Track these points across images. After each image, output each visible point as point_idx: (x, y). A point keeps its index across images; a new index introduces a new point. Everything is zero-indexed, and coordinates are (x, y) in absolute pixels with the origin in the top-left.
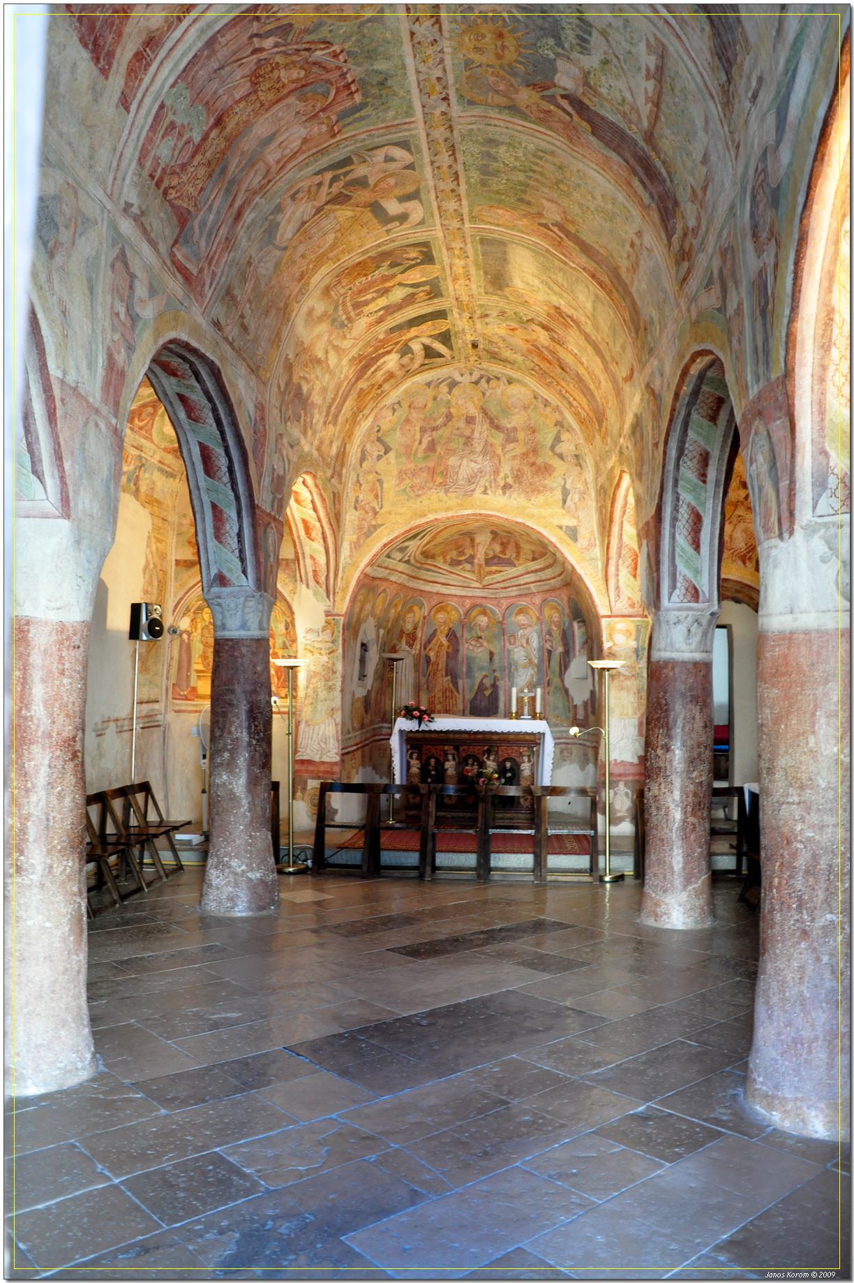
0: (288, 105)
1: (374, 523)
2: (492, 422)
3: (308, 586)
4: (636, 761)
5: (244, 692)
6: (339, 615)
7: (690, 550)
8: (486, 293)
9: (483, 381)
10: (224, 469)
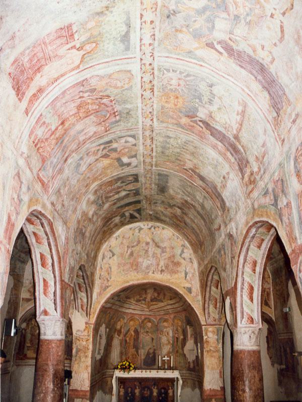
0: (90, 119)
1: (107, 285)
3: (78, 311)
4: (219, 389)
5: (53, 365)
6: (91, 324)
7: (249, 301)
8: (157, 194)
9: (153, 228)
10: (50, 264)
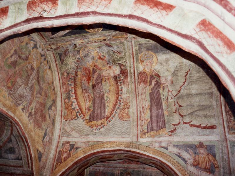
2: (38, 78)
9: (43, 58)
